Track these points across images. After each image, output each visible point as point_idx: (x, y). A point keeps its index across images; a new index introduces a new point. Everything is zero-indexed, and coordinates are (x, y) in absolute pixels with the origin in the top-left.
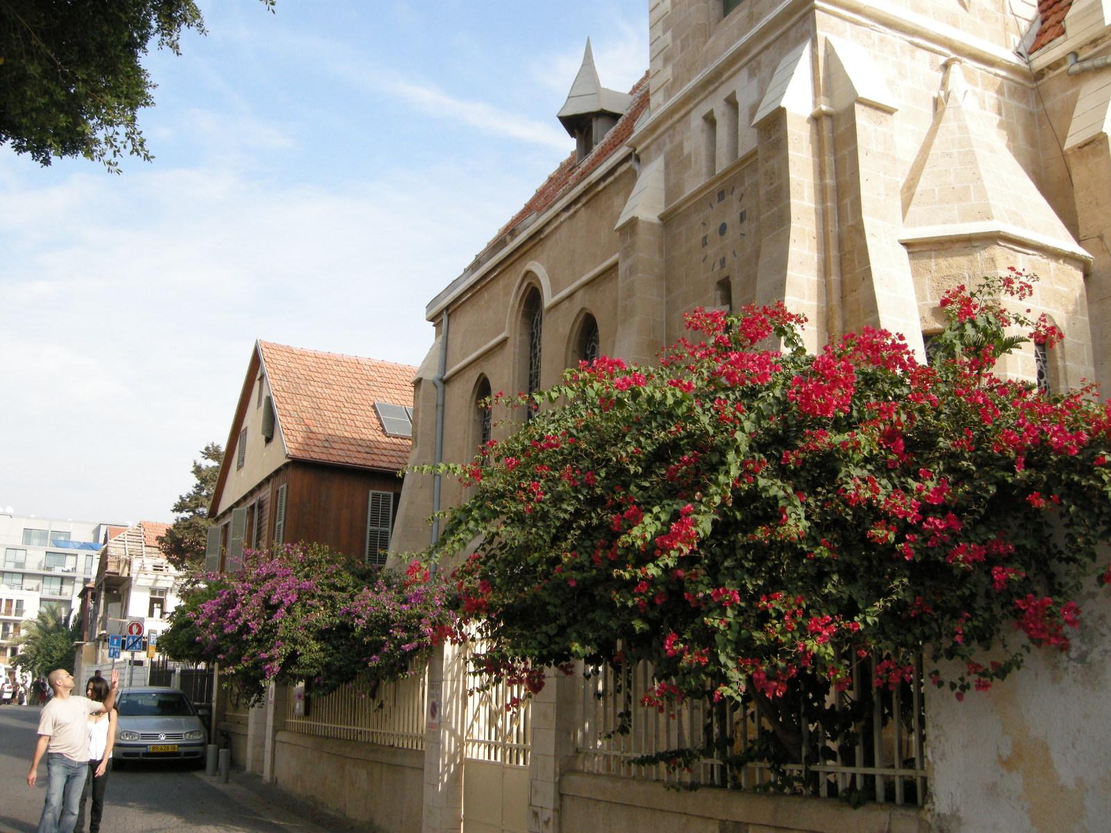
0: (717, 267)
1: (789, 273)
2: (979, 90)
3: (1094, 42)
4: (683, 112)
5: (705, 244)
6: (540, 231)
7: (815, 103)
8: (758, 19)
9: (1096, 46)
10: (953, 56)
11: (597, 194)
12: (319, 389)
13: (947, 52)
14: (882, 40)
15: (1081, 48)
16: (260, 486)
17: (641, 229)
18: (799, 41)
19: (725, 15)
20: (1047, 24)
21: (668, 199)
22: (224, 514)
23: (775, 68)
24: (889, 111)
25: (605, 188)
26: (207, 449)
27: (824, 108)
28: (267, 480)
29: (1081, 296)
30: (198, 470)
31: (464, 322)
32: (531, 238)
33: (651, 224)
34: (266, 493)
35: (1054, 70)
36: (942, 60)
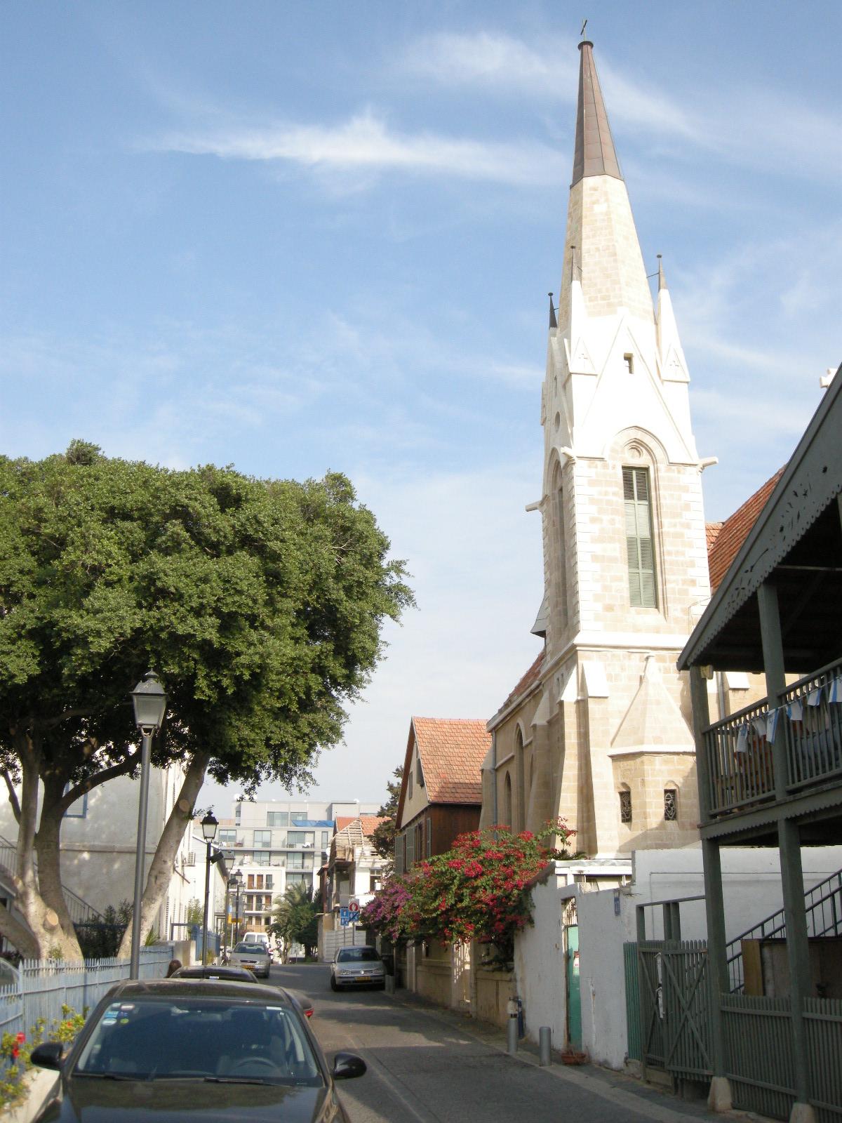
1: (564, 773)
12: (451, 750)
16: (419, 815)
21: (551, 714)
22: (404, 828)
24: (606, 698)
26: (397, 770)
28: (422, 812)
29: (692, 769)
30: (391, 788)
31: (501, 738)
33: (543, 726)
34: (422, 820)
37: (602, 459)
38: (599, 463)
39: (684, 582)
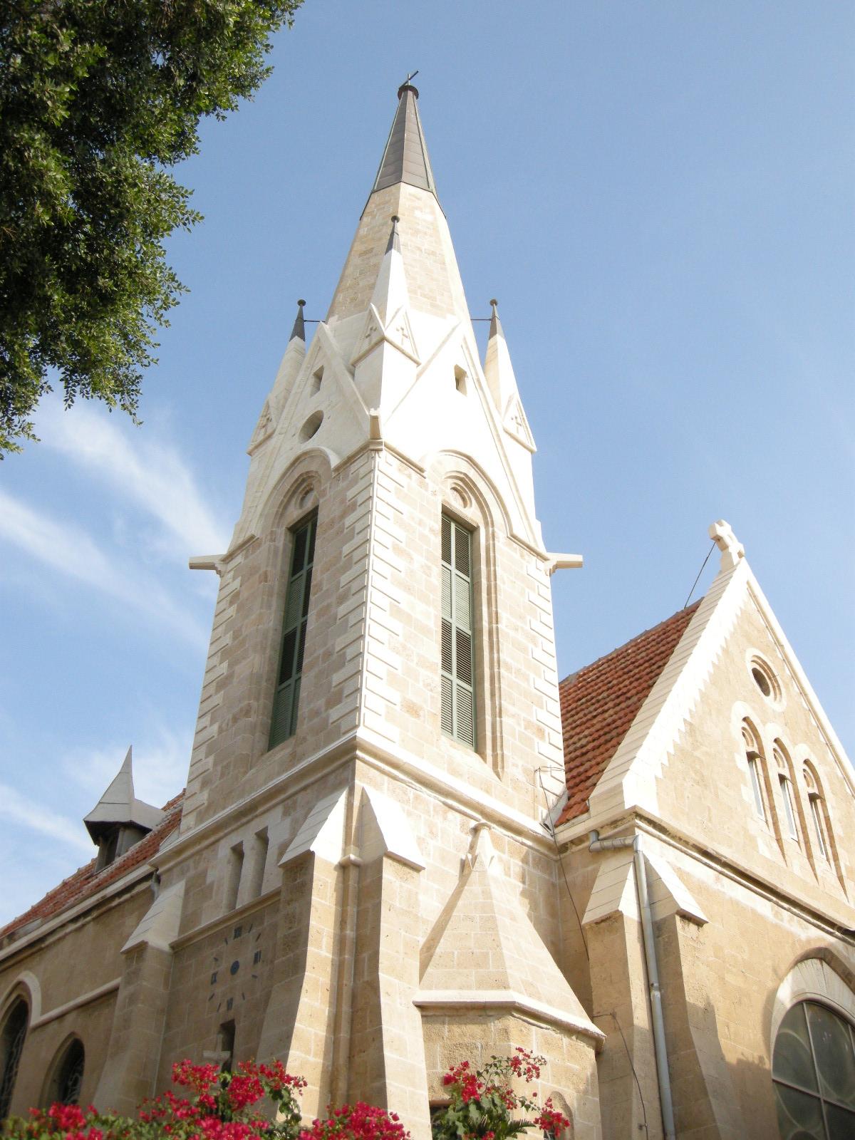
0: (224, 1008)
1: (297, 1025)
2: (506, 857)
3: (614, 823)
4: (212, 839)
5: (214, 981)
6: (41, 939)
7: (345, 852)
8: (300, 760)
9: (615, 827)
10: (483, 821)
11: (110, 909)
13: (479, 817)
14: (417, 798)
15: (602, 828)
17: (149, 955)
18: (337, 787)
19: (269, 750)
20: (573, 801)
21: (183, 928)
23: (310, 810)
24: (416, 868)
25: (119, 904)
27: (353, 857)
29: (592, 1075)
32: (31, 945)
33: (160, 952)
35: (577, 845)
36: (473, 824)
37: (420, 470)
38: (415, 476)
39: (528, 725)
